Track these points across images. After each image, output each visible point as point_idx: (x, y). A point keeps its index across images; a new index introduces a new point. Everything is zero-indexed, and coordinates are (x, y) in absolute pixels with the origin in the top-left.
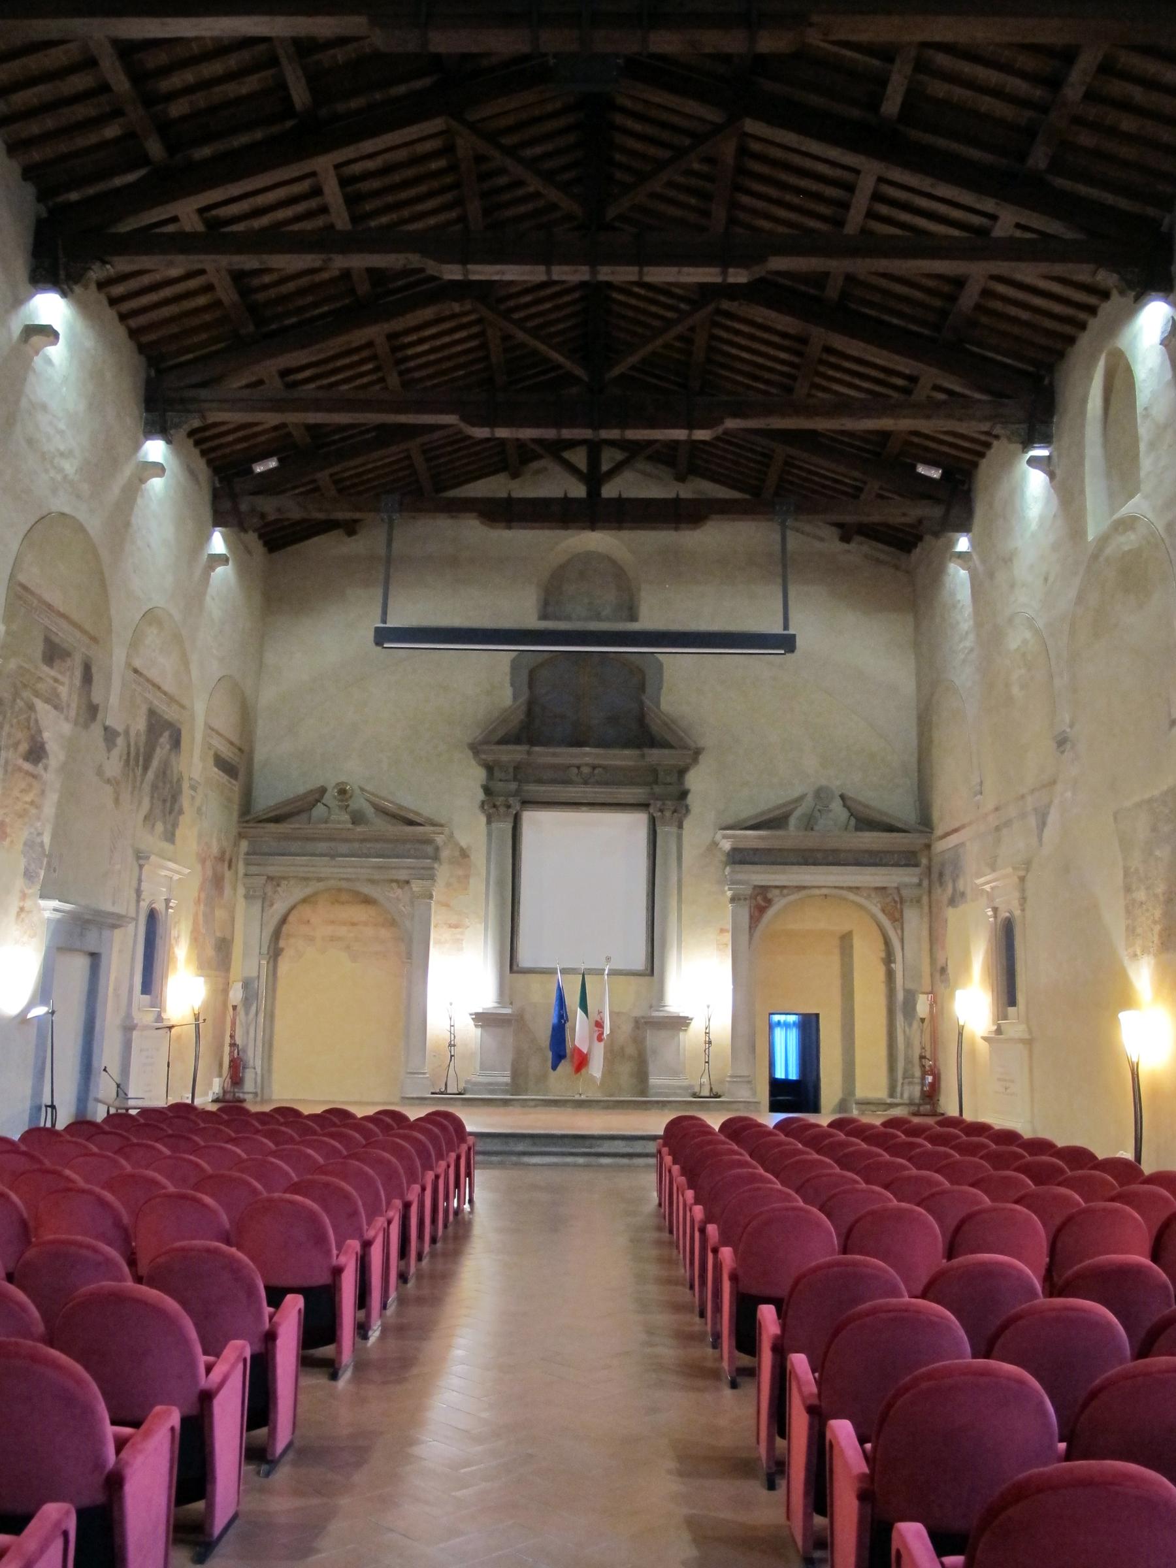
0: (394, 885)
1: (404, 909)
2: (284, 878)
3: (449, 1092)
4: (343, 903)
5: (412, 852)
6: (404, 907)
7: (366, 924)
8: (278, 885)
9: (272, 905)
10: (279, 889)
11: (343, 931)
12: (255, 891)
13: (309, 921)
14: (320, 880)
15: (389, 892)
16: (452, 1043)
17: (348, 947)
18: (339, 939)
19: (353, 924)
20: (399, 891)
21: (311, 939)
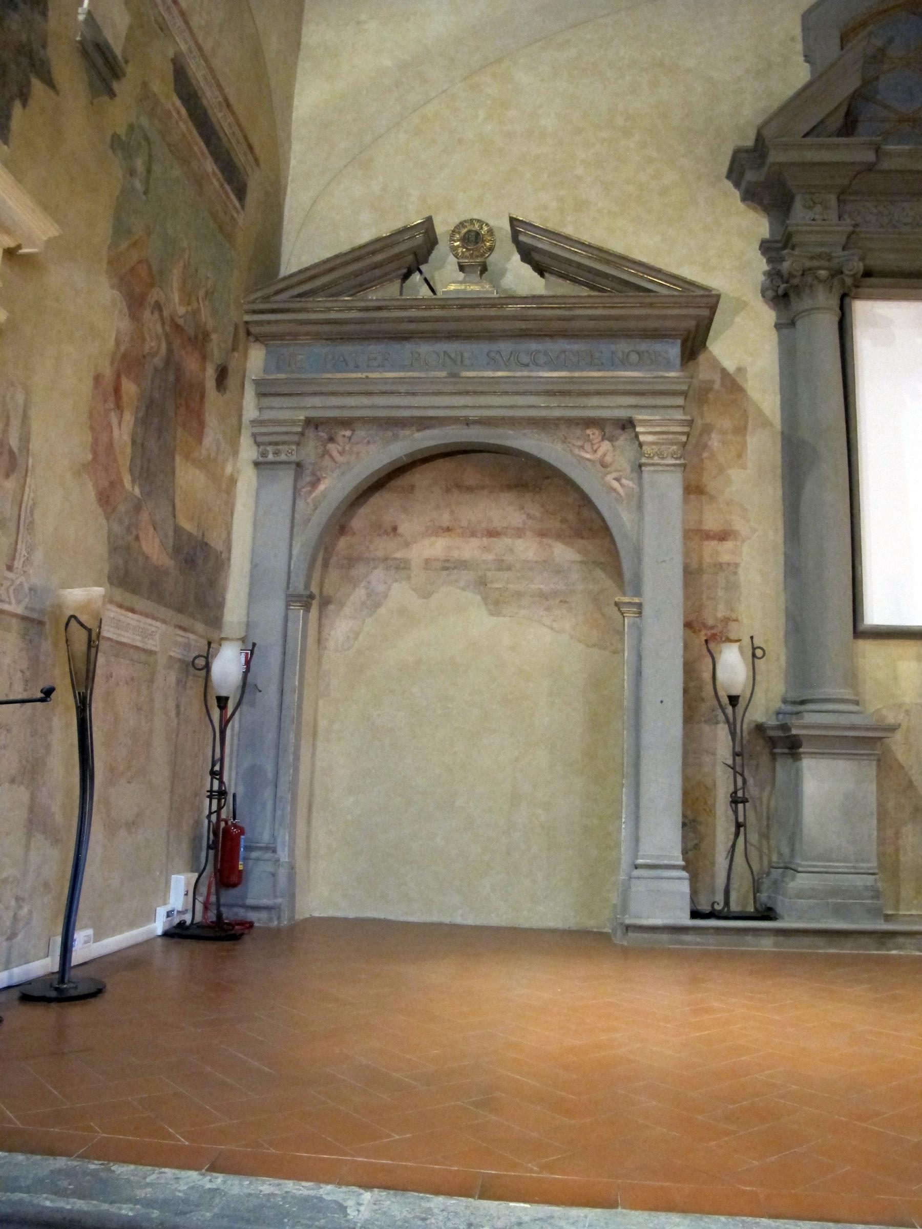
0: (594, 433)
1: (616, 485)
2: (346, 423)
3: (734, 907)
4: (470, 489)
5: (634, 357)
6: (617, 480)
7: (519, 533)
8: (331, 439)
9: (314, 484)
10: (331, 447)
11: (470, 549)
12: (276, 453)
13: (395, 529)
14: (424, 423)
15: (582, 447)
16: (740, 794)
17: (482, 583)
18: (463, 564)
19: (493, 533)
20: (606, 446)
21: (401, 567)
